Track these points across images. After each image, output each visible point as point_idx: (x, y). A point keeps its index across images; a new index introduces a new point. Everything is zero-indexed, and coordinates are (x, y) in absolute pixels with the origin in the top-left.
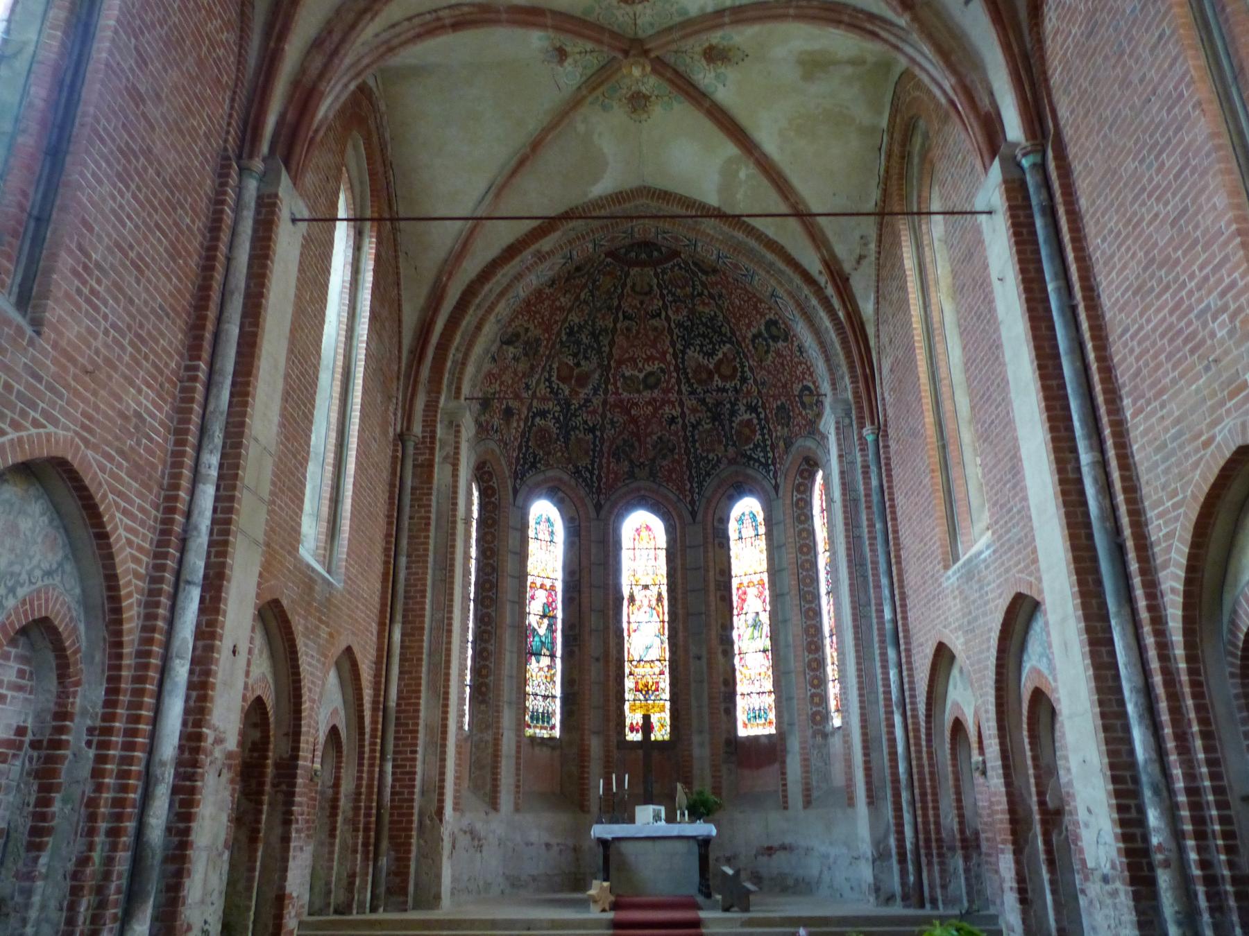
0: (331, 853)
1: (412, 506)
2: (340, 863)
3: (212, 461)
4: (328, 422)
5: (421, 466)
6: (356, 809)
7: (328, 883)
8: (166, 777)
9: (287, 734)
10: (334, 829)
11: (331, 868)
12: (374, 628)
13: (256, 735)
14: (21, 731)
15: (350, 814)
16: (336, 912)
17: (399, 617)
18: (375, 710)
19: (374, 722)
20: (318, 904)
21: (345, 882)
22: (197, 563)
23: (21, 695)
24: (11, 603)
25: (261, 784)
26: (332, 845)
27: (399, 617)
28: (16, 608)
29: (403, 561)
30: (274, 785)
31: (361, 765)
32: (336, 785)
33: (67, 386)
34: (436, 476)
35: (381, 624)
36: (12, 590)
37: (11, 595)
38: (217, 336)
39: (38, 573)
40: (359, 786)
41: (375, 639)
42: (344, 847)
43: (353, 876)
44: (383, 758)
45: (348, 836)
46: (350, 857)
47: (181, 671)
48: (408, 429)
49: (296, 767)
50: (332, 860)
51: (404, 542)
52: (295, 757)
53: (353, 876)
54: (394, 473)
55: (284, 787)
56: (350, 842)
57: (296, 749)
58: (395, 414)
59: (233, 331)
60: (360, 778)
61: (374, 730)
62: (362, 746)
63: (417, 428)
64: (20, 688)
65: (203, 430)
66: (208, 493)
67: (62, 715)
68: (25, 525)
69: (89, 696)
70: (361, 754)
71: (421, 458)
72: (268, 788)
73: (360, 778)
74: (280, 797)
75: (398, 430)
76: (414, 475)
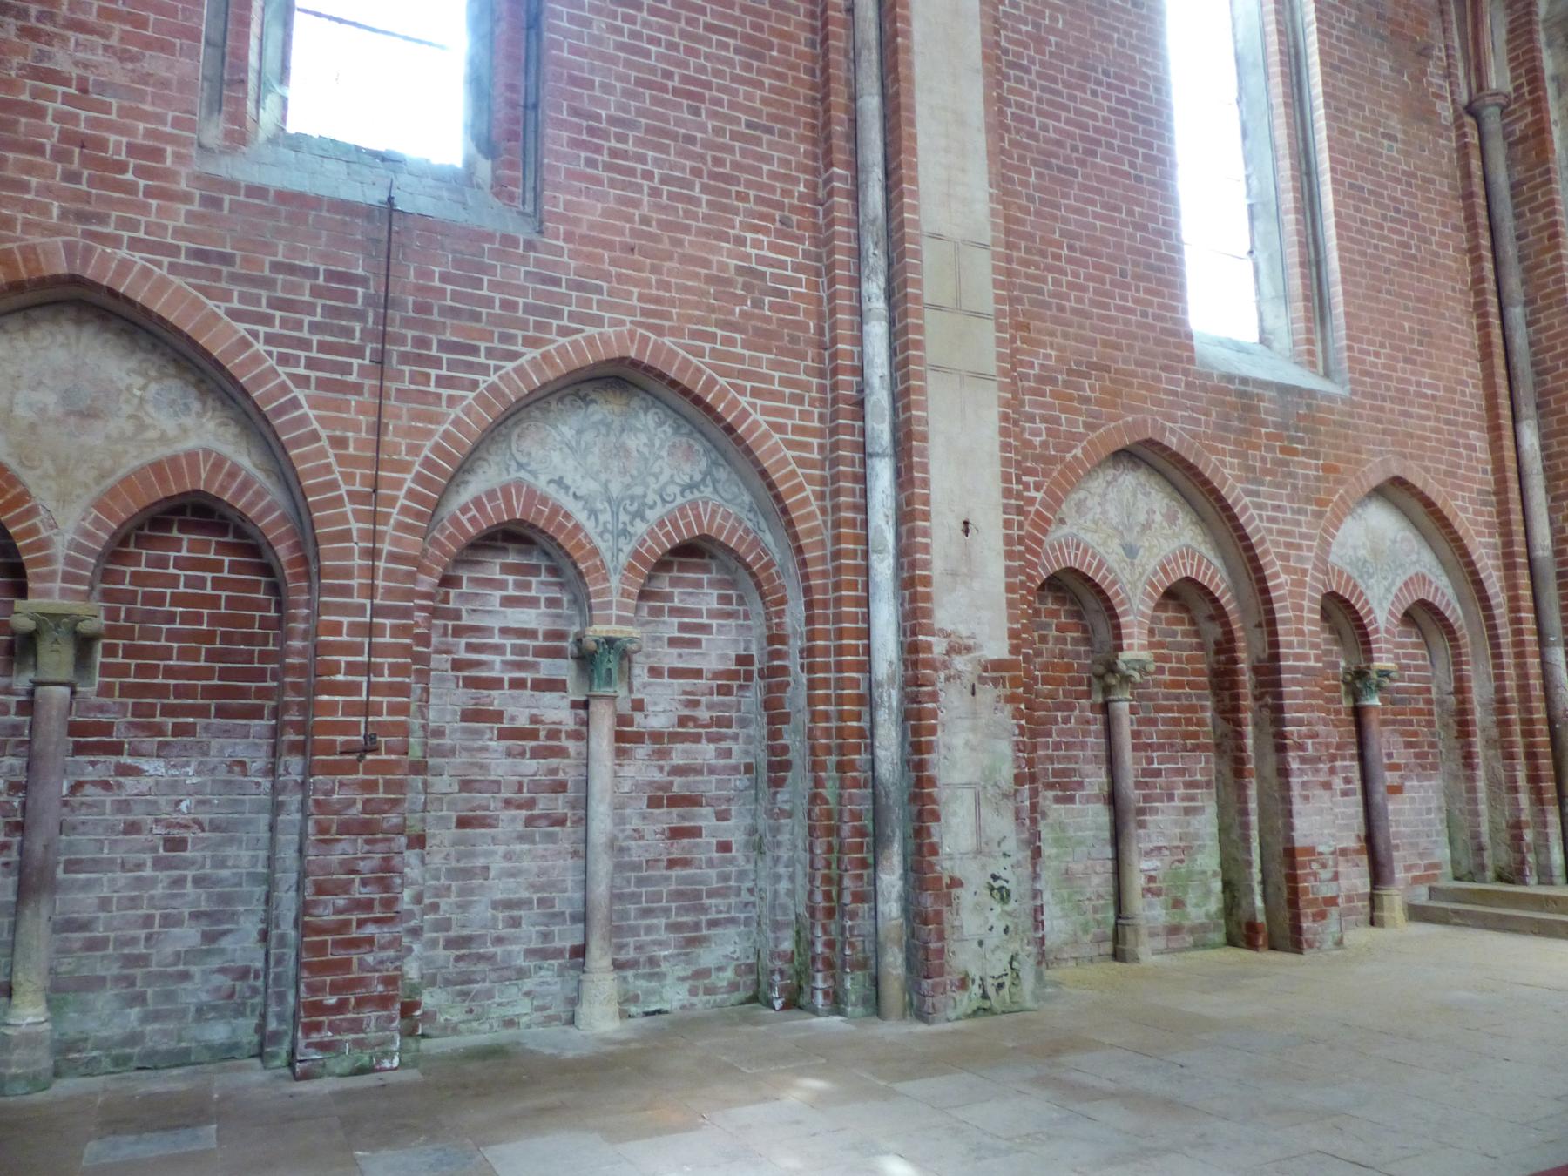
0: (1472, 790)
1: (1518, 216)
2: (1492, 807)
3: (874, 288)
4: (1274, 147)
5: (1524, 139)
6: (1504, 724)
7: (1476, 836)
8: (890, 699)
9: (1259, 625)
10: (1468, 758)
11: (1476, 814)
12: (1478, 439)
13: (1214, 631)
14: (744, 660)
15: (1494, 733)
16: (1500, 878)
17: (1528, 409)
18: (1509, 566)
19: (1512, 587)
20: (1467, 863)
21: (1505, 836)
22: (880, 429)
23: (732, 622)
24: (640, 528)
25: (1236, 697)
26: (1471, 779)
27: (1528, 409)
28: (651, 533)
29: (1517, 313)
30: (1257, 698)
31: (1497, 656)
32: (1461, 689)
33: (606, 276)
34: (1557, 145)
35: (1495, 429)
36: (639, 514)
37: (638, 521)
38: (854, 122)
39: (673, 489)
40: (1500, 689)
41: (1484, 455)
42: (1493, 782)
43: (1517, 826)
44: (1542, 641)
45: (1498, 766)
46: (1506, 797)
47: (883, 568)
48: (1480, 88)
49: (1278, 671)
50: (1474, 801)
51: (1513, 283)
52: (1275, 657)
53: (1517, 826)
54: (1467, 175)
55: (1269, 700)
56: (1502, 775)
57: (1275, 644)
58: (1448, 75)
59: (871, 103)
60: (1500, 677)
61: (1514, 600)
62: (1492, 627)
63: (1499, 78)
64: (729, 615)
65: (858, 254)
66: (877, 332)
67: (776, 638)
68: (635, 442)
69: (794, 615)
70: (1494, 640)
71: (1519, 128)
72: (1247, 702)
73: (1500, 677)
74: (1266, 713)
75: (1464, 98)
76: (1511, 162)
